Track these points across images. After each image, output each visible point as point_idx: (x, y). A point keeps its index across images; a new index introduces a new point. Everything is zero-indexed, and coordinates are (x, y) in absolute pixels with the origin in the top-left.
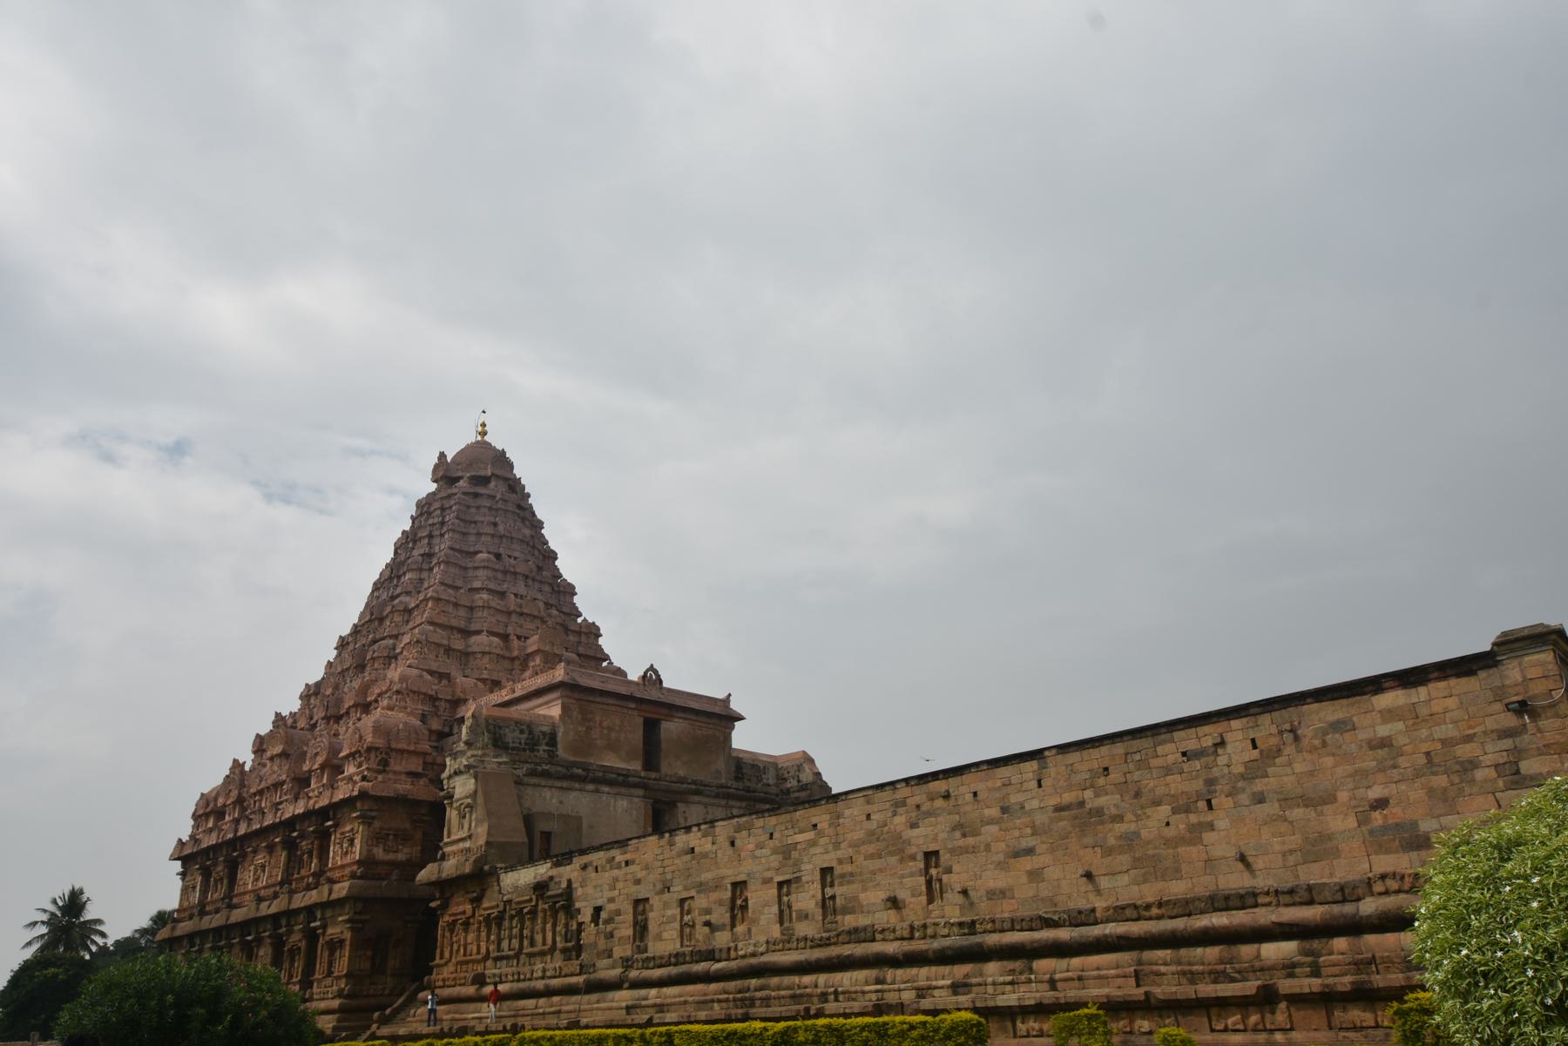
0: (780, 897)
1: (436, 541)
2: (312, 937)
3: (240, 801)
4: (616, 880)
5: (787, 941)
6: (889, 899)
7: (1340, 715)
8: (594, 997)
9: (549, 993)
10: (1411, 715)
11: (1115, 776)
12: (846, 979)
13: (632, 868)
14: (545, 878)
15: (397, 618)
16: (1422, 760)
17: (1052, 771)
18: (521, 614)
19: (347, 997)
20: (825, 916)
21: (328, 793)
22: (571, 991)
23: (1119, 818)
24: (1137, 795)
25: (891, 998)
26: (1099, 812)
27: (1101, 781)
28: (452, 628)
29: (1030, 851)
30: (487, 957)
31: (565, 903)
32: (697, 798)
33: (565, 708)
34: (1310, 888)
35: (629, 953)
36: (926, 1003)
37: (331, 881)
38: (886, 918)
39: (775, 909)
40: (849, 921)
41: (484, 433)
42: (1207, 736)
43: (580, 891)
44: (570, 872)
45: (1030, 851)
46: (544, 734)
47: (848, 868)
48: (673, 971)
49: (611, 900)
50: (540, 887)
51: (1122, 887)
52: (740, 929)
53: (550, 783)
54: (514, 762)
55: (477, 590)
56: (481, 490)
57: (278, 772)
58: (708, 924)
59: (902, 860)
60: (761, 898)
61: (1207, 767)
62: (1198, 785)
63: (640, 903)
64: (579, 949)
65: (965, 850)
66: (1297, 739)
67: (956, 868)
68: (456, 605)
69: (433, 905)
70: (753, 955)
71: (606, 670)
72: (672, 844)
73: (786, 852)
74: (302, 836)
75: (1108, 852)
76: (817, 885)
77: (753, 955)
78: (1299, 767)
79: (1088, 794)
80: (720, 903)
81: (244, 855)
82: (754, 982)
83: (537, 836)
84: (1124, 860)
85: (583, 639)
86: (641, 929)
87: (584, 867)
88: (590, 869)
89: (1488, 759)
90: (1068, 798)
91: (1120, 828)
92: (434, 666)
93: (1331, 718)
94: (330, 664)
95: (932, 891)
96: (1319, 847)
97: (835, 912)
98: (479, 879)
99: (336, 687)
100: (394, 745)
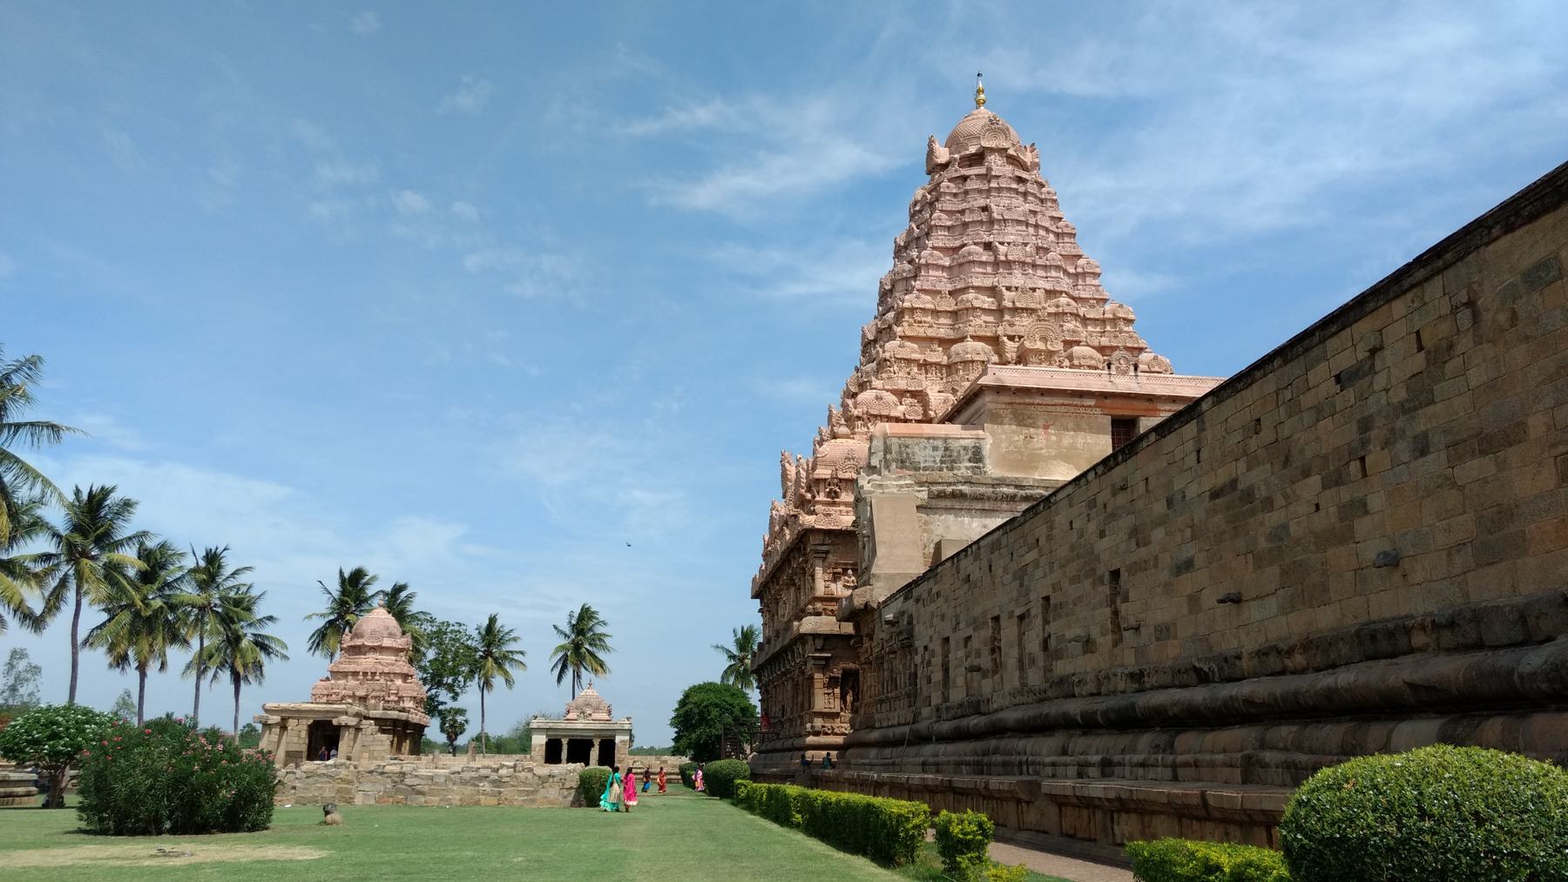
7: (1541, 252)
8: (913, 750)
11: (1267, 435)
13: (941, 600)
17: (1209, 434)
23: (1268, 504)
26: (1249, 495)
27: (1253, 443)
28: (932, 339)
29: (1188, 565)
31: (908, 646)
34: (1478, 616)
39: (1015, 652)
40: (1062, 668)
43: (917, 629)
45: (1188, 565)
46: (965, 448)
51: (1269, 621)
53: (966, 505)
54: (921, 484)
58: (978, 669)
59: (1094, 584)
61: (1362, 398)
62: (1351, 433)
66: (1476, 317)
67: (1132, 595)
73: (1021, 575)
75: (1260, 561)
76: (1039, 621)
78: (1477, 376)
82: (993, 743)
84: (1273, 572)
86: (946, 671)
90: (1222, 477)
91: (1274, 518)
92: (902, 384)
93: (1527, 262)
100: (841, 475)
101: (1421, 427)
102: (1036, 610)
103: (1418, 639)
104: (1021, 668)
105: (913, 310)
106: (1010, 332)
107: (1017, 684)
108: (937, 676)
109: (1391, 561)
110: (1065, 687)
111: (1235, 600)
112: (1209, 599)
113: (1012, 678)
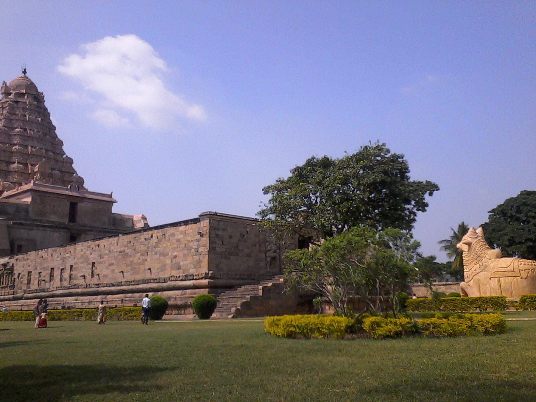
5: (62, 287)
6: (82, 276)
10: (185, 233)
11: (132, 244)
12: (70, 299)
13: (28, 261)
14: (6, 263)
16: (184, 245)
17: (120, 240)
20: (70, 280)
23: (130, 256)
26: (127, 254)
27: (129, 245)
29: (113, 264)
31: (11, 271)
32: (90, 233)
35: (25, 289)
38: (81, 281)
39: (59, 277)
40: (75, 282)
41: (25, 72)
43: (15, 268)
44: (13, 261)
45: (113, 264)
47: (76, 266)
49: (23, 271)
51: (128, 276)
55: (15, 145)
58: (44, 280)
60: (57, 273)
62: (146, 248)
67: (98, 268)
70: (53, 291)
73: (64, 259)
75: (127, 266)
76: (69, 271)
78: (164, 245)
79: (126, 248)
84: (130, 268)
86: (29, 281)
87: (17, 260)
88: (18, 260)
89: (194, 247)
90: (122, 249)
91: (131, 259)
104: (61, 280)
107: (59, 285)
109: (150, 269)
110: (76, 286)
111: (122, 272)
112: (117, 271)
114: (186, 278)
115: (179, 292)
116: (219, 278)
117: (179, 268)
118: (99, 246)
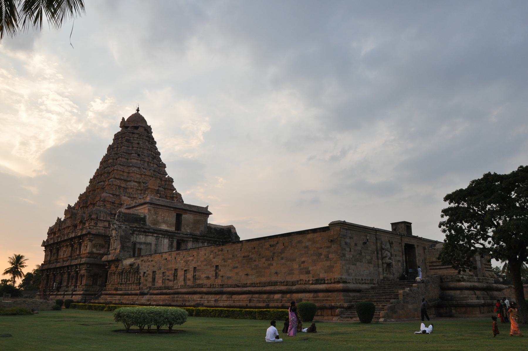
0: (185, 274)
1: (119, 149)
2: (77, 273)
3: (59, 230)
4: (149, 265)
9: (132, 294)
11: (256, 250)
12: (196, 297)
13: (153, 262)
15: (106, 175)
18: (145, 175)
19: (85, 291)
21: (80, 232)
22: (136, 294)
23: (255, 261)
24: (260, 255)
25: (202, 302)
26: (251, 259)
27: (253, 251)
28: (122, 179)
29: (237, 267)
30: (118, 284)
31: (137, 271)
33: (149, 210)
34: (287, 282)
36: (209, 304)
37: (81, 258)
38: (205, 282)
39: (183, 277)
40: (198, 282)
41: (138, 110)
42: (275, 241)
43: (141, 267)
44: (139, 261)
45: (237, 267)
47: (199, 268)
48: (159, 291)
49: (147, 271)
50: (131, 265)
51: (253, 279)
52: (175, 282)
56: (136, 131)
57: (69, 223)
58: (168, 280)
60: (180, 273)
62: (271, 254)
63: (154, 272)
64: (140, 283)
65: (224, 266)
68: (123, 172)
69: (107, 267)
70: (177, 289)
71: (173, 194)
72: (162, 256)
73: (187, 262)
74: (74, 243)
75: (252, 269)
76: (193, 272)
77: (177, 289)
79: (250, 254)
80: (171, 274)
81: (61, 247)
82: (176, 296)
83: (137, 250)
85: (167, 183)
86: (154, 279)
87: (142, 261)
89: (324, 253)
90: (246, 254)
91: (256, 263)
94: (87, 188)
95: (216, 276)
96: (291, 272)
97: (196, 280)
98: (117, 261)
99: (87, 197)
101: (282, 256)
102: (192, 269)
103: (278, 284)
104: (184, 280)
105: (117, 170)
106: (144, 181)
108: (150, 280)
109: (276, 273)
110: (201, 286)
111: (247, 275)
113: (181, 282)
114: (318, 281)
115: (311, 295)
116: (349, 283)
117: (308, 272)
118: (222, 250)
